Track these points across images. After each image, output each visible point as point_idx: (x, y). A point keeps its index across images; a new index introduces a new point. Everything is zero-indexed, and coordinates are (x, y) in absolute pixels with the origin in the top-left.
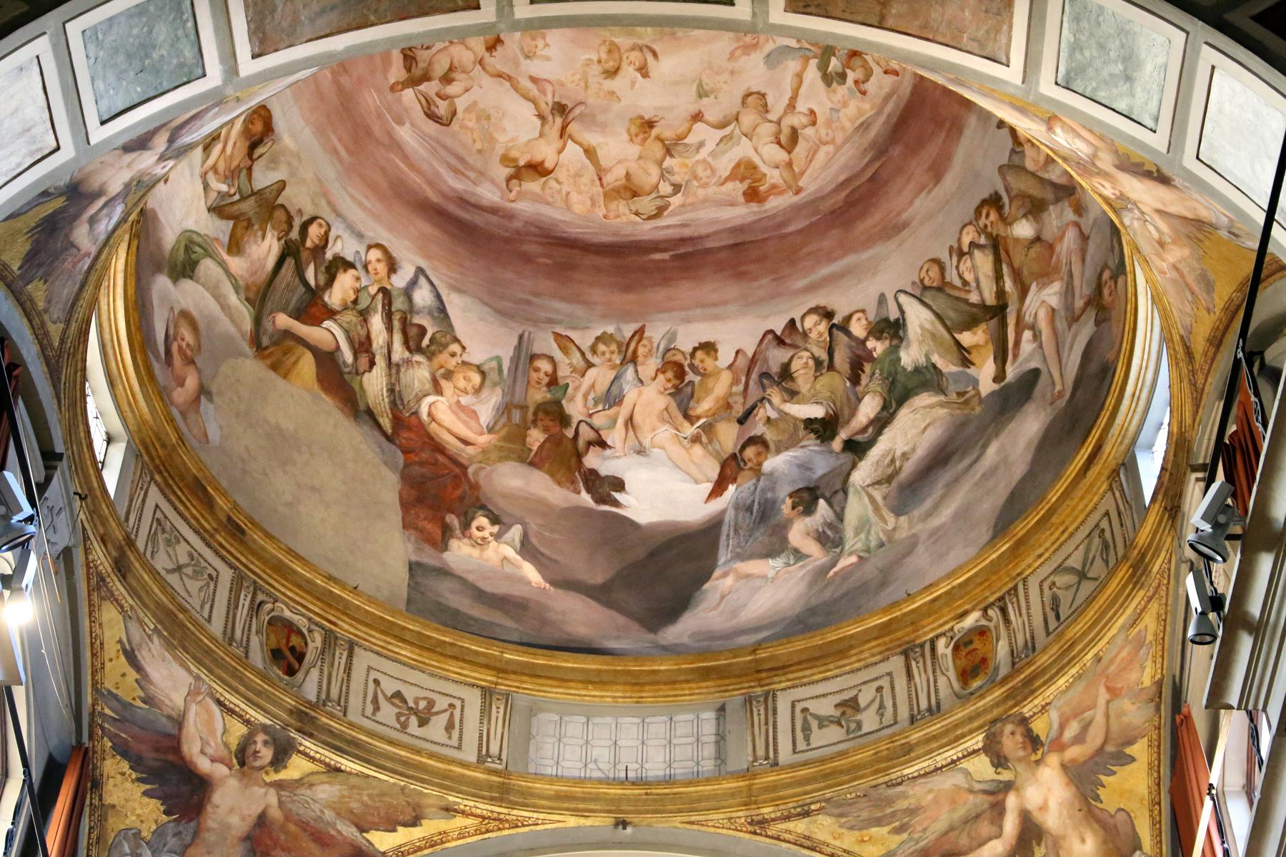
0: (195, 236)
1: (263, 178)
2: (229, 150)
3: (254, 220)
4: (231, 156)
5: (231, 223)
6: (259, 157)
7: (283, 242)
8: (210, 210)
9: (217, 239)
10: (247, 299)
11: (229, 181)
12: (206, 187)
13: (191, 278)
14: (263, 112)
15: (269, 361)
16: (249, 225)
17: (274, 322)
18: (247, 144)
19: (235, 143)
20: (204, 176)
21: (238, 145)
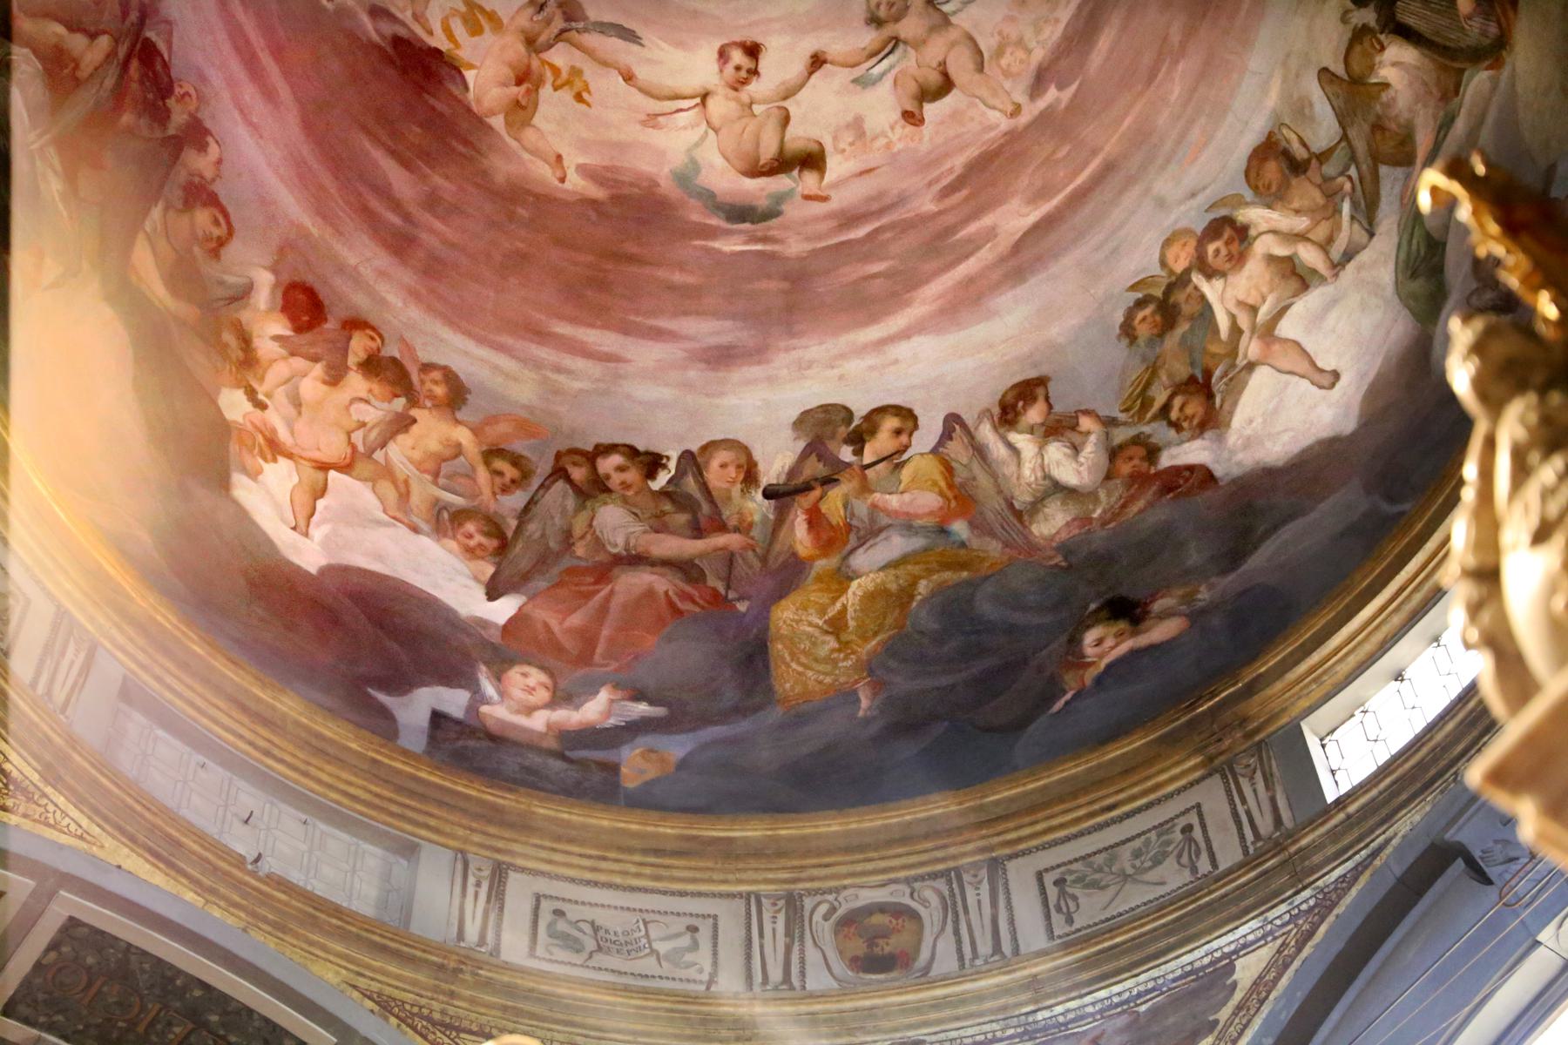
0: (1403, 256)
1: (1323, 129)
2: (1302, 223)
3: (1372, 118)
4: (1310, 211)
5: (1384, 170)
6: (1304, 145)
7: (1382, 37)
8: (1372, 235)
9: (1402, 199)
10: (1457, 93)
11: (1337, 198)
12: (1348, 256)
13: (1445, 244)
14: (1253, 175)
15: (1511, 14)
16: (1378, 127)
17: (1469, 17)
18: (1294, 182)
19: (1297, 212)
20: (1337, 266)
21: (1296, 205)
